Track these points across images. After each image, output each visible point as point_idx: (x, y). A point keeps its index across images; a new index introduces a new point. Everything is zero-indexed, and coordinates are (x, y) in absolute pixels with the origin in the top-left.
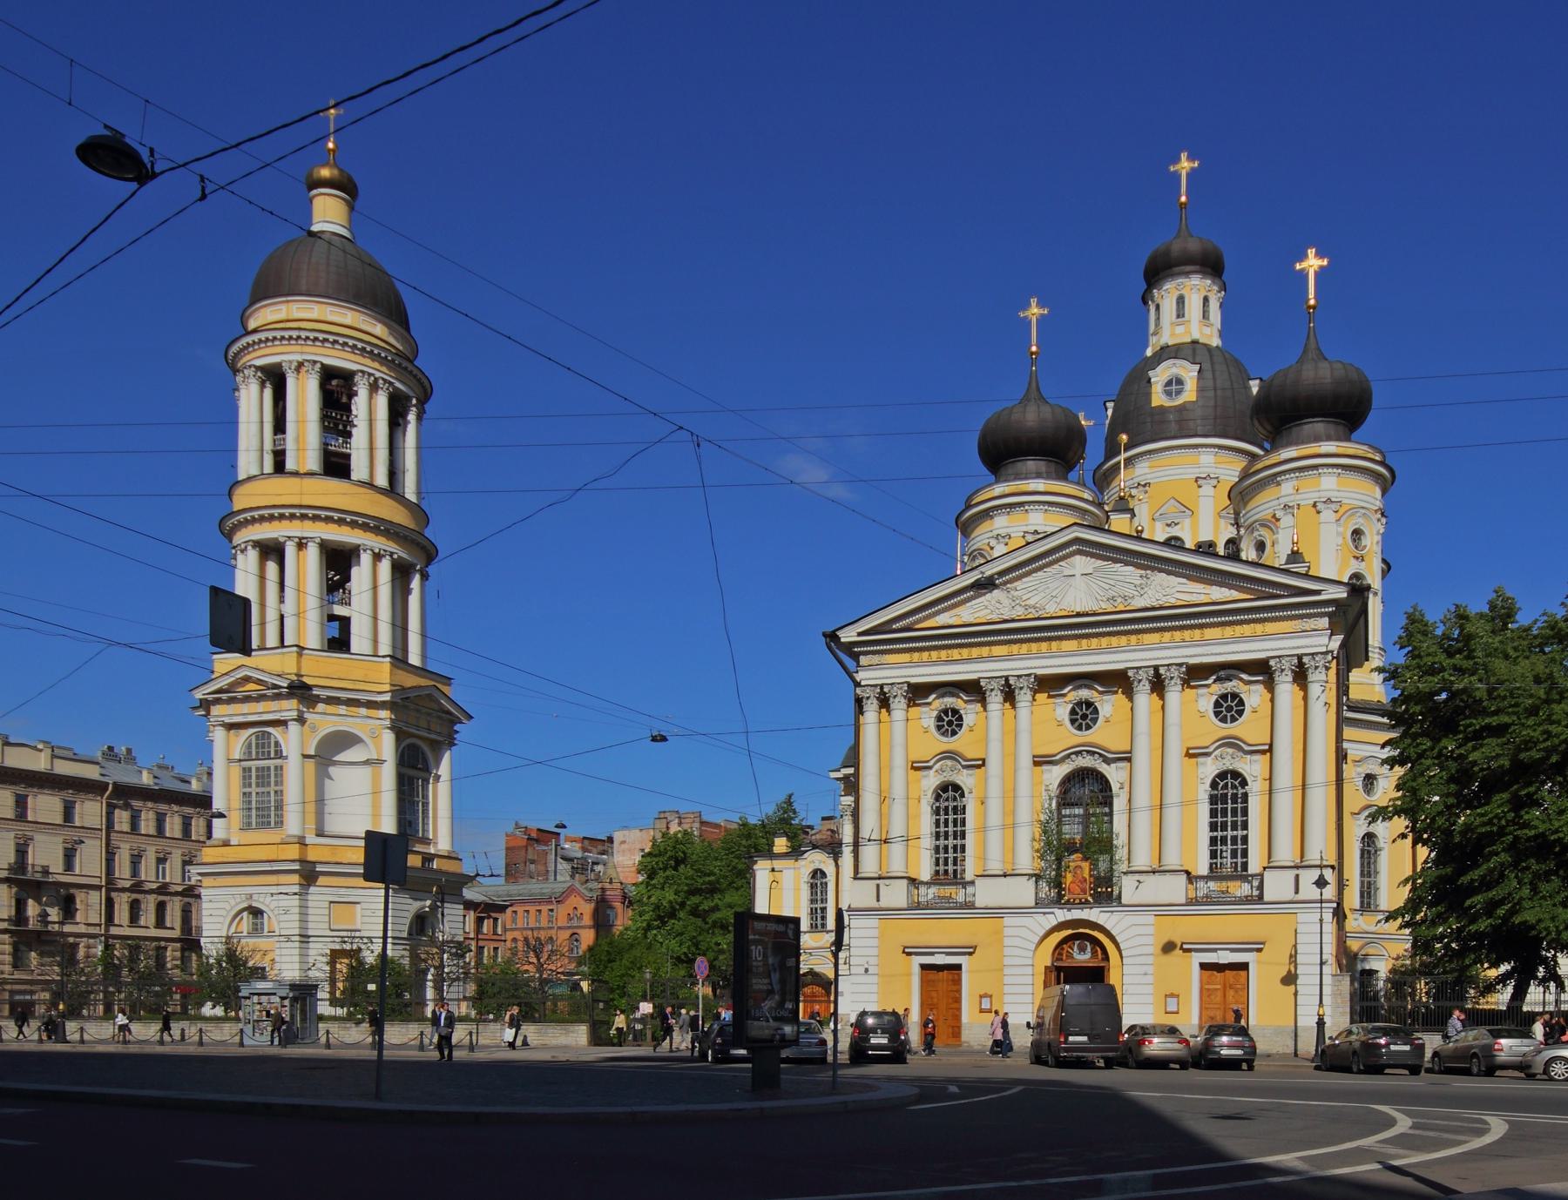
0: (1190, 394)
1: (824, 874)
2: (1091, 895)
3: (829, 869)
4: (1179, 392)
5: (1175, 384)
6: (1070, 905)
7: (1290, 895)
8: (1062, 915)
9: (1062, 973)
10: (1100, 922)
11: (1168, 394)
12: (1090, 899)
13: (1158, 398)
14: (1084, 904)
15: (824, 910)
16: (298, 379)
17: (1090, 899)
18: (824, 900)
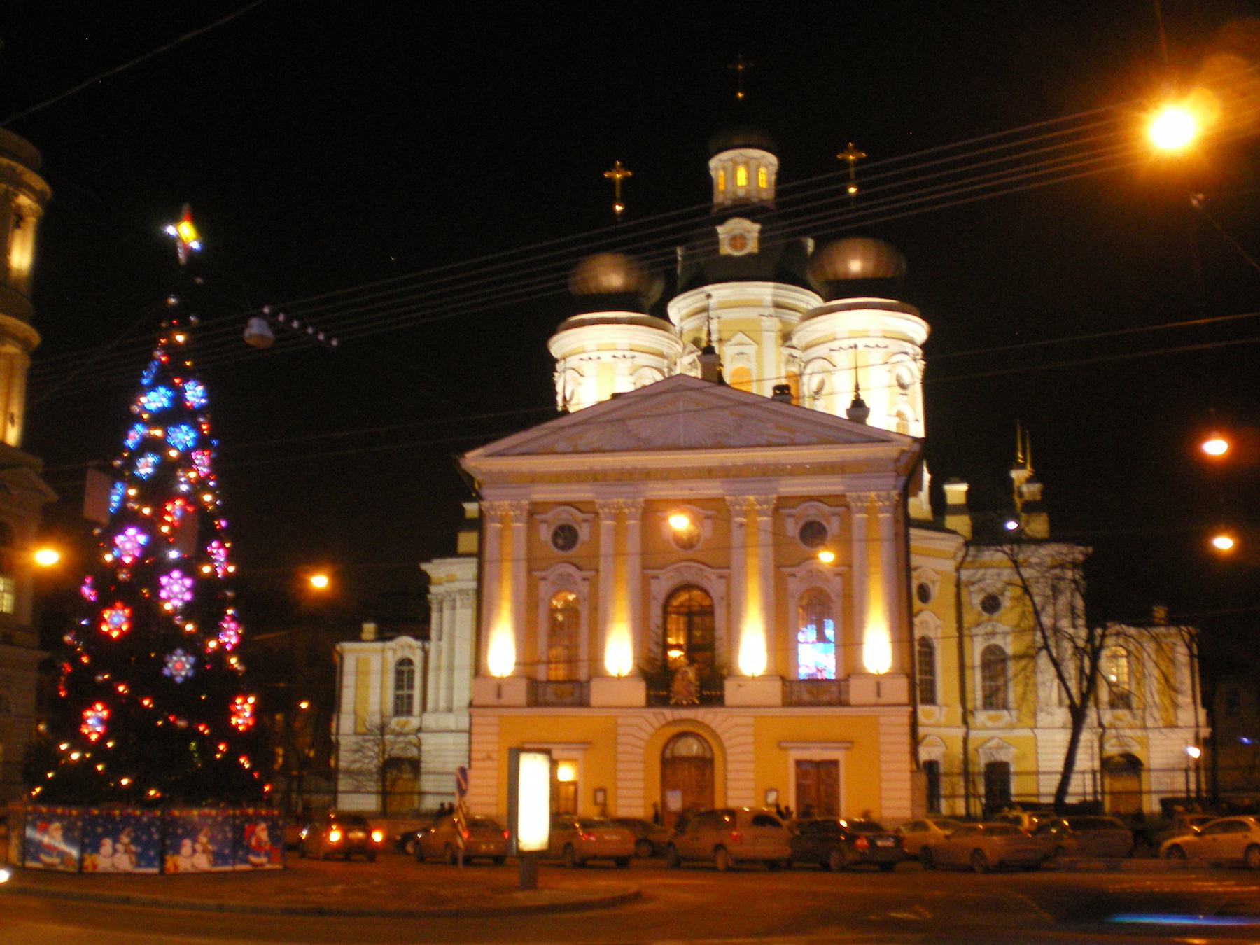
0: (752, 247)
1: (410, 662)
2: (697, 698)
3: (417, 658)
4: (743, 246)
5: (738, 240)
6: (678, 705)
7: (872, 699)
8: (669, 714)
9: (670, 765)
10: (707, 721)
11: (734, 247)
12: (697, 702)
13: (726, 249)
14: (692, 705)
15: (410, 697)
16: (564, 359)
17: (697, 702)
18: (411, 687)
